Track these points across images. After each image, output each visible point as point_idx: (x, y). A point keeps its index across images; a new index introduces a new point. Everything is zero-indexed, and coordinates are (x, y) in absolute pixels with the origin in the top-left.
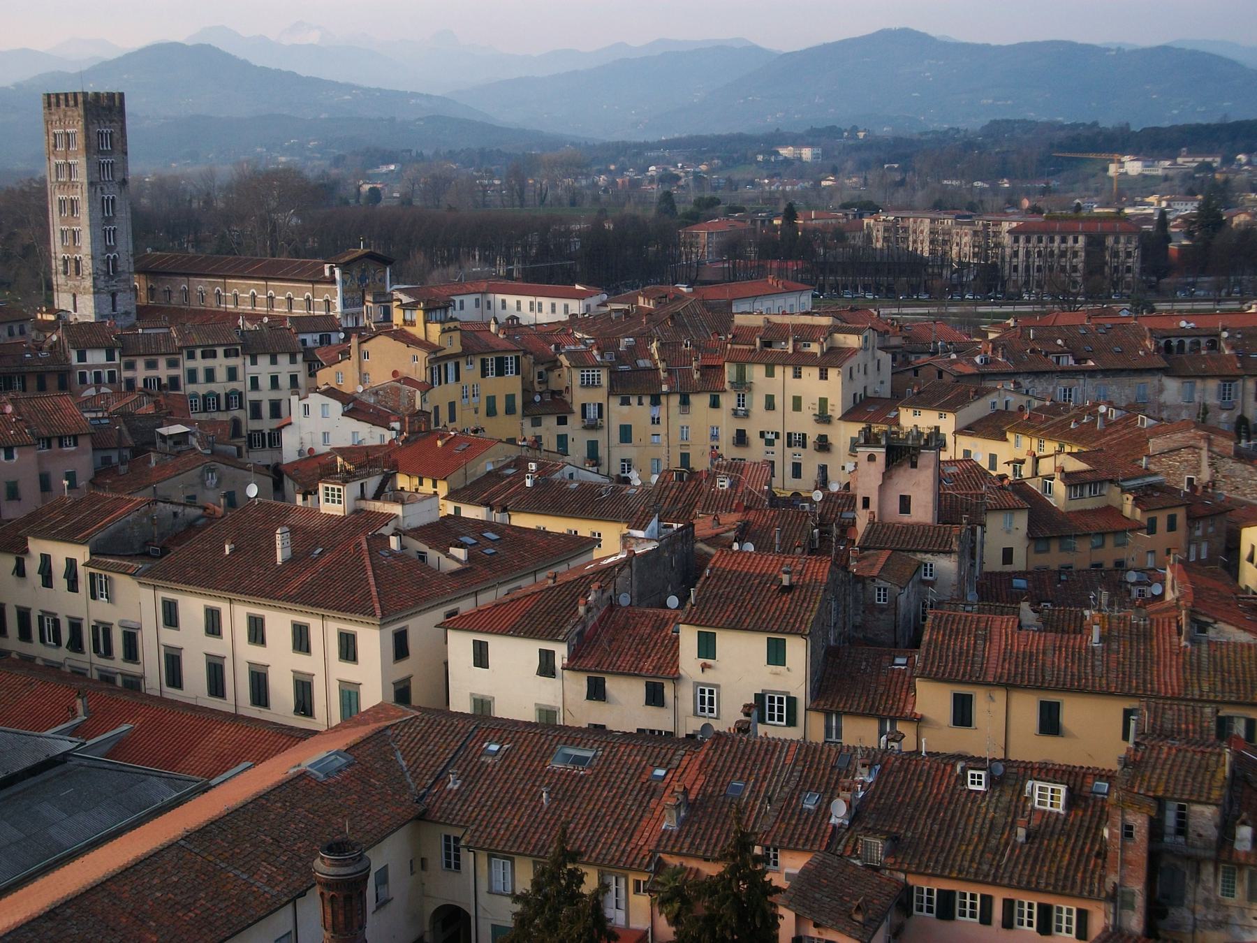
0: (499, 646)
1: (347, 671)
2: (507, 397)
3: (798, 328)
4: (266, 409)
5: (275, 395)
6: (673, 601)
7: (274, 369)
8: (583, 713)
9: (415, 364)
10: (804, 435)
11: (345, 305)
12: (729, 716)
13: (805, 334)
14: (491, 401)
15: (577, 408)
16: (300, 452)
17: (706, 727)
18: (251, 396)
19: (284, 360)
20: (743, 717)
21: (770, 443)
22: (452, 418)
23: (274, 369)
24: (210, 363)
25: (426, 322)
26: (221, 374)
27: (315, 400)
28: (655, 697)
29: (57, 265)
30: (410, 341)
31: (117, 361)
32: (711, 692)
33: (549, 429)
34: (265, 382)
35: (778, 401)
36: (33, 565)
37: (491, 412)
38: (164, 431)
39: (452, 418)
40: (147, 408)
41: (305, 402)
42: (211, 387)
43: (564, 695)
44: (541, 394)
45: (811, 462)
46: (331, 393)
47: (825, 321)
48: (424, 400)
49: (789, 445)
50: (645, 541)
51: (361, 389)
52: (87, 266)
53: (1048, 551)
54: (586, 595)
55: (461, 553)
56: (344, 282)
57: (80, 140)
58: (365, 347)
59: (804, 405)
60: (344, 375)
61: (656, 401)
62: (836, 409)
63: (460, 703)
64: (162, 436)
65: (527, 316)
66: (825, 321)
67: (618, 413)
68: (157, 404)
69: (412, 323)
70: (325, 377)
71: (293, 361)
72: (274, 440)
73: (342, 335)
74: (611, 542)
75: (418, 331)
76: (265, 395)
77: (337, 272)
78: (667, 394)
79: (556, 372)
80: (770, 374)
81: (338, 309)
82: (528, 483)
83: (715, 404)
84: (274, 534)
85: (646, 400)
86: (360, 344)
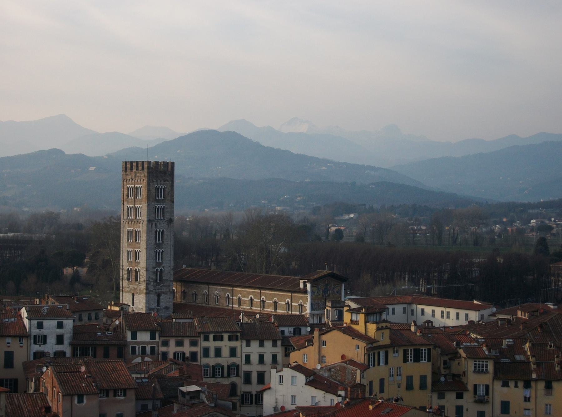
5: (261, 368)
7: (261, 350)
9: (357, 351)
11: (313, 308)
14: (410, 379)
15: (470, 387)
16: (275, 409)
18: (245, 368)
19: (268, 344)
22: (382, 390)
23: (261, 350)
24: (218, 344)
25: (366, 322)
26: (225, 352)
27: (287, 373)
29: (123, 274)
30: (355, 334)
31: (157, 340)
33: (450, 401)
34: (255, 359)
37: (409, 387)
38: (184, 389)
39: (382, 390)
40: (175, 373)
42: (219, 360)
44: (445, 376)
46: (299, 368)
48: (362, 377)
51: (319, 367)
56: (313, 292)
57: (144, 193)
58: (324, 337)
60: (307, 356)
61: (527, 385)
64: (182, 392)
67: (500, 392)
68: (181, 370)
69: (357, 323)
70: (295, 357)
71: (275, 345)
72: (258, 399)
73: (309, 329)
75: (360, 328)
76: (254, 368)
77: (309, 286)
78: (536, 380)
79: (457, 361)
81: (308, 311)
85: (521, 384)
86: (320, 335)
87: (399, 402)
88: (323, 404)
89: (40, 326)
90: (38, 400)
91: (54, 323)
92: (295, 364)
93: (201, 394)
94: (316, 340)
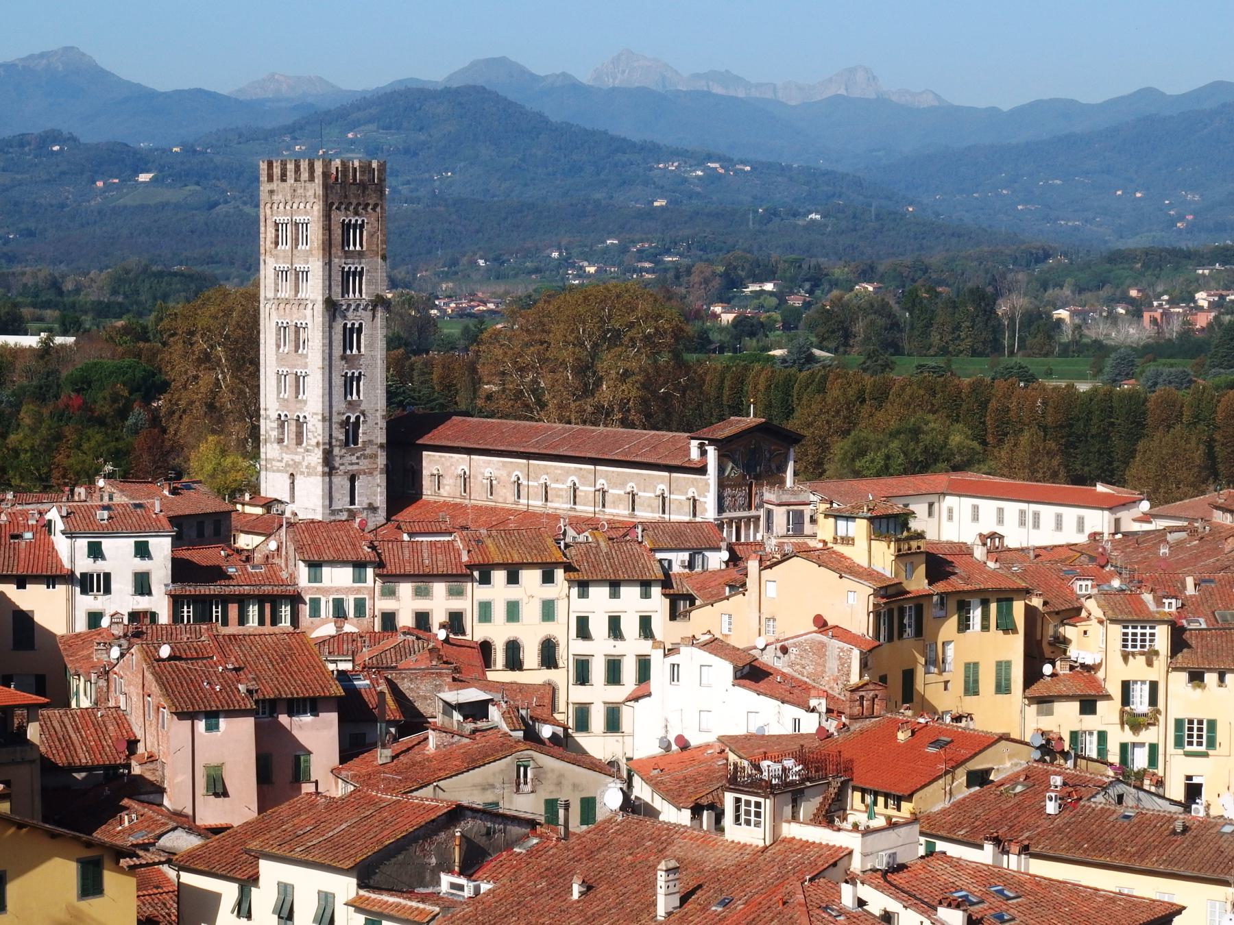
2: (999, 664)
4: (598, 671)
7: (615, 606)
9: (854, 608)
11: (721, 509)
15: (1115, 690)
18: (580, 647)
23: (615, 606)
24: (513, 592)
26: (531, 611)
27: (690, 658)
29: (268, 427)
30: (844, 568)
33: (1065, 718)
34: (599, 627)
36: (264, 898)
37: (972, 688)
46: (715, 645)
48: (864, 666)
52: (316, 430)
57: (315, 233)
65: (1015, 537)
67: (1182, 701)
69: (848, 541)
70: (704, 619)
75: (857, 554)
76: (600, 647)
77: (712, 452)
81: (709, 512)
82: (1051, 808)
84: (654, 868)
87: (963, 724)
88: (774, 730)
89: (95, 552)
90: (108, 724)
91: (128, 544)
92: (708, 637)
93: (491, 708)
94: (751, 582)
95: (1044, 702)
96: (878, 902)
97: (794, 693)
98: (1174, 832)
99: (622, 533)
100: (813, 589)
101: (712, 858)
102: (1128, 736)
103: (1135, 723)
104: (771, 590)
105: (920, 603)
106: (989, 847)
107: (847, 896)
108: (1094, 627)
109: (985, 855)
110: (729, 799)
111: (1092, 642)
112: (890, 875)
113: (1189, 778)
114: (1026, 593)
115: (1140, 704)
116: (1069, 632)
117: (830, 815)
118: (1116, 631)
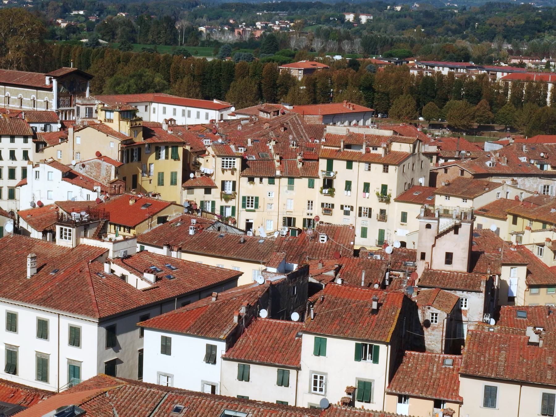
0: (178, 341)
1: (74, 353)
2: (172, 173)
3: (369, 137)
6: (295, 316)
7: (12, 146)
8: (232, 388)
10: (370, 209)
11: (58, 106)
12: (336, 395)
13: (375, 141)
14: (161, 176)
15: (219, 184)
17: (324, 401)
20: (345, 395)
21: (347, 213)
23: (12, 146)
27: (44, 169)
28: (283, 382)
30: (109, 132)
32: (321, 378)
33: (198, 195)
35: (353, 186)
37: (161, 183)
41: (37, 169)
43: (223, 377)
45: (374, 226)
46: (54, 164)
47: (388, 133)
48: (117, 173)
49: (360, 215)
50: (274, 275)
51: (74, 163)
53: (538, 294)
54: (238, 309)
55: (151, 277)
59: (371, 188)
61: (272, 180)
62: (393, 191)
63: (149, 377)
65: (180, 121)
66: (388, 133)
67: (246, 188)
69: (110, 121)
70: (50, 152)
71: (26, 142)
74: (252, 275)
77: (55, 82)
78: (280, 177)
80: (349, 166)
81: (53, 107)
82: (191, 232)
83: (311, 185)
84: (26, 257)
85: (265, 180)
87: (156, 198)
88: (79, 199)
92: (51, 160)
94: (70, 137)
95: (190, 189)
96: (119, 271)
97: (87, 184)
98: (240, 242)
99: (16, 115)
100: (96, 142)
101: (51, 253)
102: (224, 203)
103: (226, 198)
104: (78, 141)
105: (140, 147)
106: (165, 248)
107: (107, 268)
108: (210, 158)
109: (164, 252)
110: (58, 228)
111: (210, 164)
112: (125, 260)
113: (248, 220)
114: (184, 144)
115: (229, 190)
116: (201, 160)
117: (100, 235)
118: (220, 160)
